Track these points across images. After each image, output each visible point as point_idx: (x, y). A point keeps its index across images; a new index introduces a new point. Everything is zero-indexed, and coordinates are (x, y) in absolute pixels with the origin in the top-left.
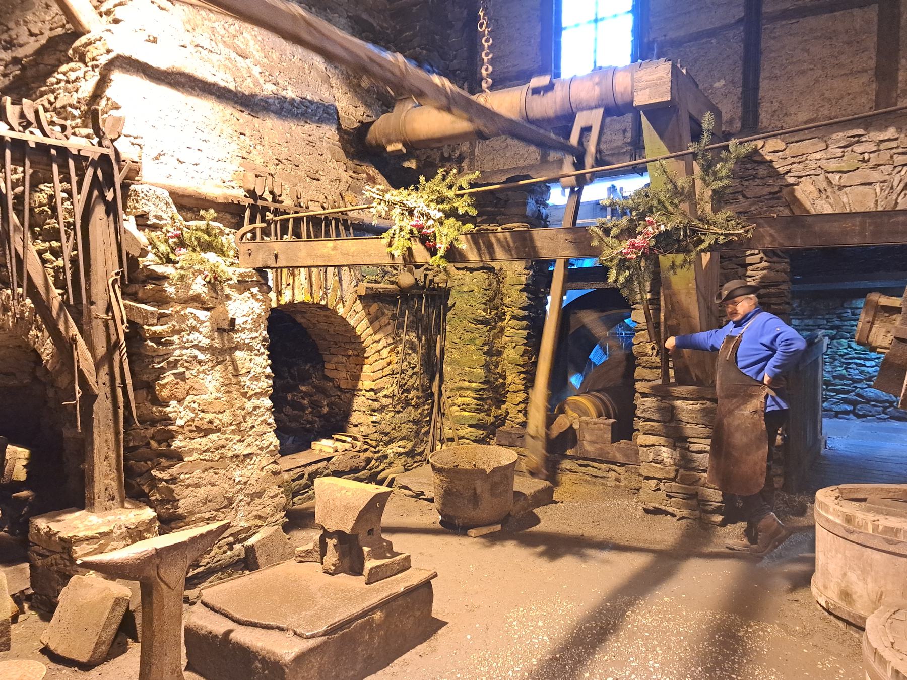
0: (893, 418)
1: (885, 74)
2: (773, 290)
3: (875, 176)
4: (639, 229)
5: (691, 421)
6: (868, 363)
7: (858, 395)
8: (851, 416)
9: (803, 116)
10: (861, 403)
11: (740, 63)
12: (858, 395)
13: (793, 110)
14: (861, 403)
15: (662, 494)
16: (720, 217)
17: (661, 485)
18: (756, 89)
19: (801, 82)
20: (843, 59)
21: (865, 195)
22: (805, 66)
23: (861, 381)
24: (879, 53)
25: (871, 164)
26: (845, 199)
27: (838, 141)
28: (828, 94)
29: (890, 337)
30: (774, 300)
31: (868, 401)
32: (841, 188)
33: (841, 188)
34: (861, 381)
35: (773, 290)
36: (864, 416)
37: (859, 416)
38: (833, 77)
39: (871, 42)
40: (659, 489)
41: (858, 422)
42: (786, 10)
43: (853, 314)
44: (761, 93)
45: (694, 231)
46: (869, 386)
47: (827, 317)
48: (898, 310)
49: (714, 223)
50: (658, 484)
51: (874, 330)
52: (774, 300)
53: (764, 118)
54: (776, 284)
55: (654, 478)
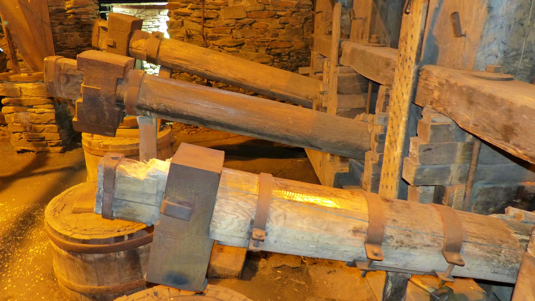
5: (33, 95)
15: (24, 140)
17: (23, 136)
40: (22, 138)
47: (152, 20)
50: (20, 135)
51: (100, 41)
55: (17, 132)
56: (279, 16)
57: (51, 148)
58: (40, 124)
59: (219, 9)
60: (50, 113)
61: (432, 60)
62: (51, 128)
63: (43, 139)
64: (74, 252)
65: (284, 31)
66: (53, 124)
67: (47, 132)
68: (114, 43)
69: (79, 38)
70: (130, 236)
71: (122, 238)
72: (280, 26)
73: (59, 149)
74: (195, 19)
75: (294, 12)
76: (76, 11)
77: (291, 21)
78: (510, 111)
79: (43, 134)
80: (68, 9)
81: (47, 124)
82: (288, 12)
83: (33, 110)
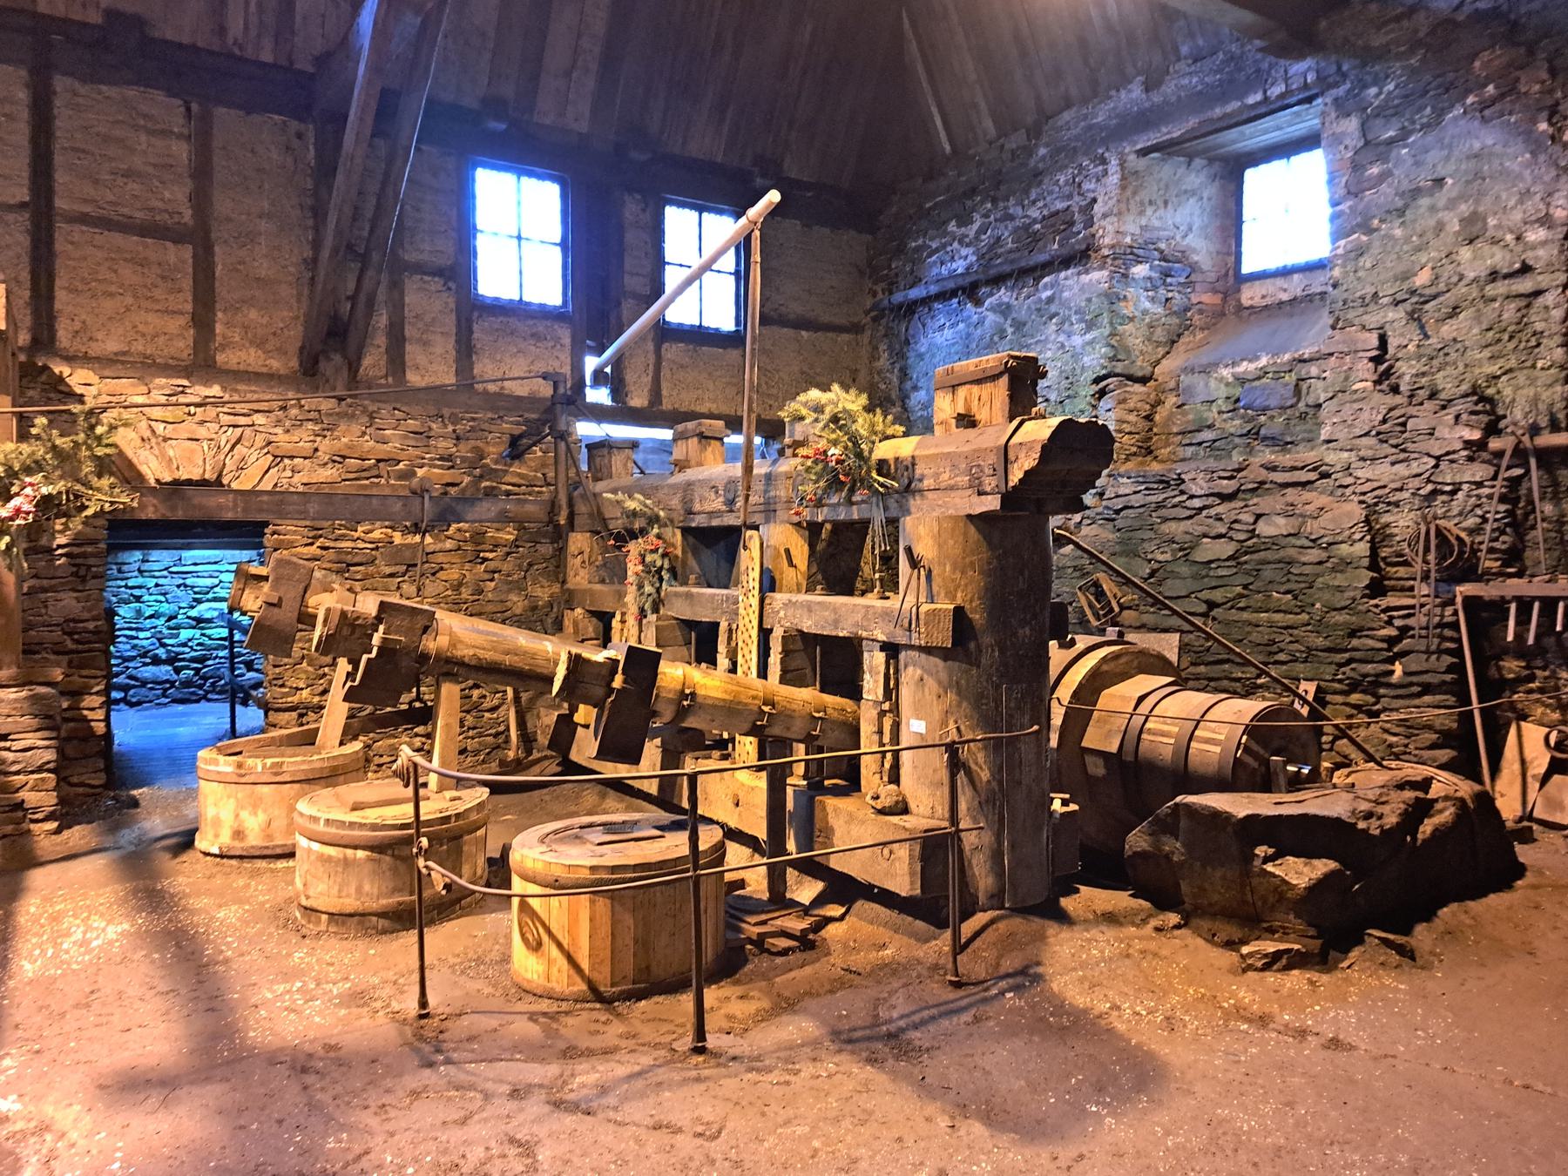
0: (175, 701)
1: (202, 321)
2: (89, 549)
3: (202, 432)
4: (14, 489)
6: (142, 635)
7: (130, 677)
8: (122, 706)
9: (112, 346)
10: (134, 687)
11: (26, 259)
12: (130, 677)
13: (100, 336)
14: (134, 687)
16: (105, 482)
18: (51, 298)
19: (108, 305)
20: (157, 293)
21: (193, 451)
22: (113, 289)
23: (133, 658)
24: (196, 299)
25: (197, 418)
26: (171, 453)
27: (162, 388)
28: (141, 328)
29: (259, 602)
30: (92, 561)
31: (144, 683)
32: (165, 440)
33: (165, 440)
34: (133, 658)
35: (89, 549)
36: (139, 703)
37: (132, 705)
38: (147, 310)
39: (187, 284)
41: (132, 711)
42: (87, 214)
43: (120, 571)
44: (57, 305)
45: (77, 497)
46: (145, 664)
48: (266, 578)
49: (98, 490)
52: (92, 561)
53: (63, 336)
54: (93, 542)
56: (485, 560)
57: (32, 826)
58: (18, 773)
59: (377, 548)
60: (47, 747)
61: (773, 590)
62: (43, 779)
63: (20, 805)
64: (378, 848)
65: (493, 584)
66: (49, 771)
67: (32, 790)
68: (280, 599)
69: (74, 602)
70: (458, 815)
71: (449, 817)
72: (487, 576)
73: (53, 825)
74: (328, 565)
75: (508, 554)
76: (76, 550)
77: (505, 567)
78: (835, 610)
79: (22, 795)
80: (59, 547)
81: (32, 772)
82: (500, 552)
83: (8, 744)
